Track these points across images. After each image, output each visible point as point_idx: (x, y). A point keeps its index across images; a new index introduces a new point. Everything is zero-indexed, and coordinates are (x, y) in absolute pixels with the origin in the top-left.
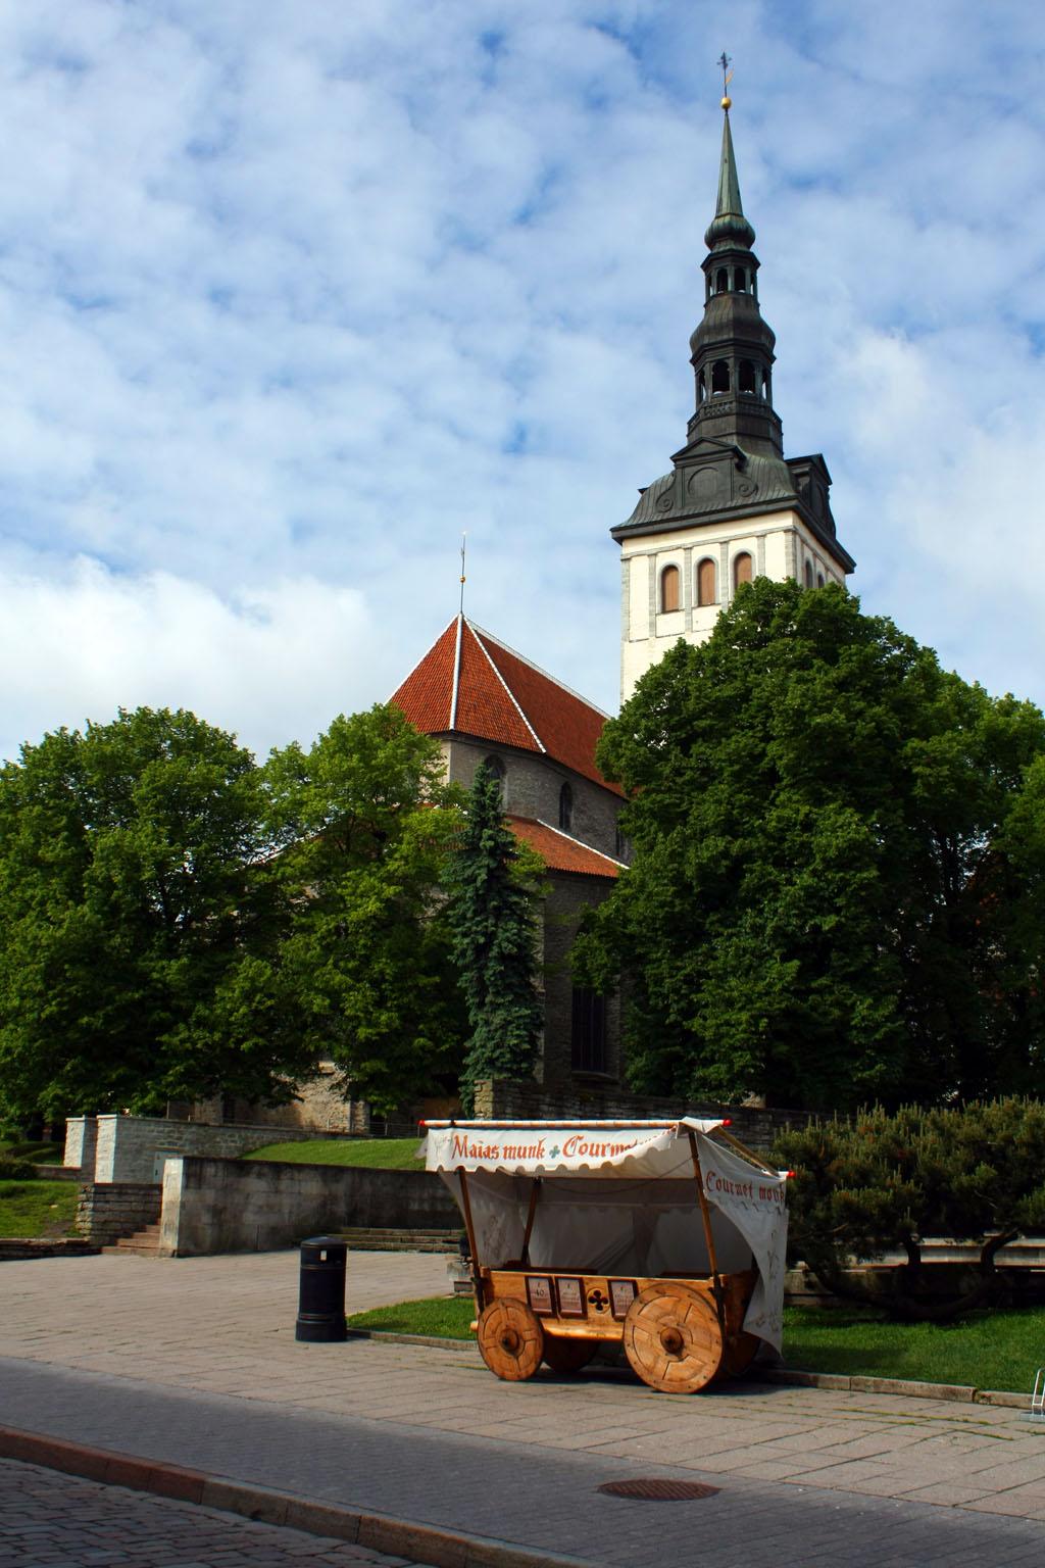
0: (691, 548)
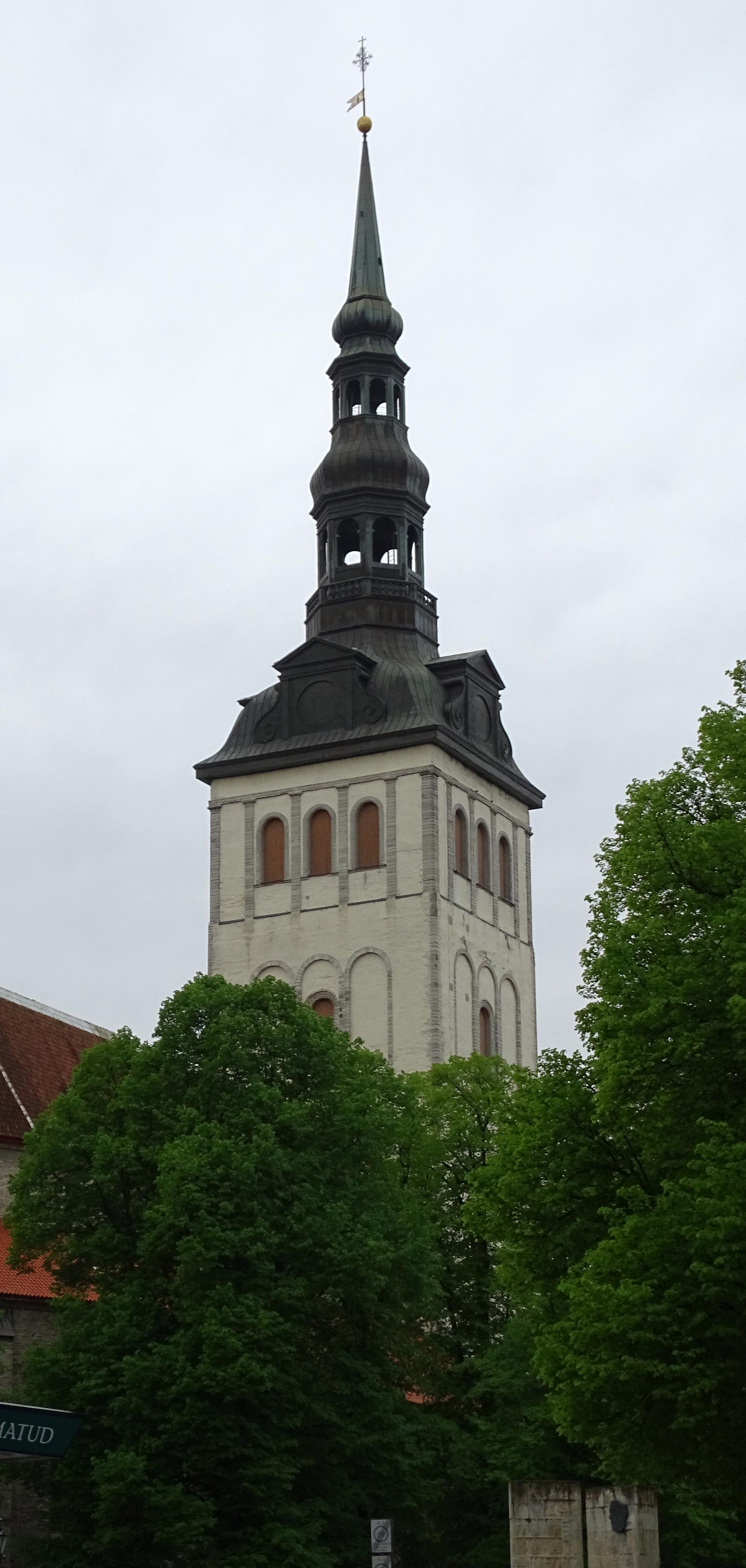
0: (299, 795)
